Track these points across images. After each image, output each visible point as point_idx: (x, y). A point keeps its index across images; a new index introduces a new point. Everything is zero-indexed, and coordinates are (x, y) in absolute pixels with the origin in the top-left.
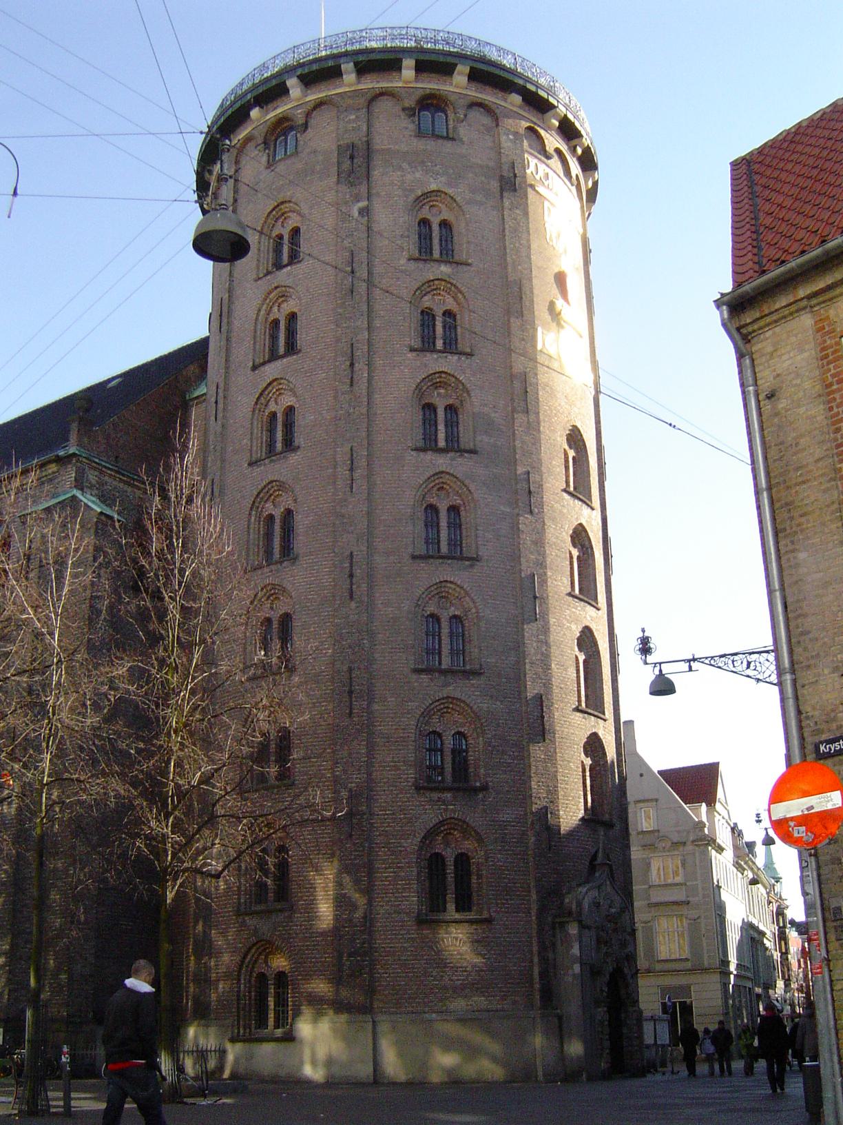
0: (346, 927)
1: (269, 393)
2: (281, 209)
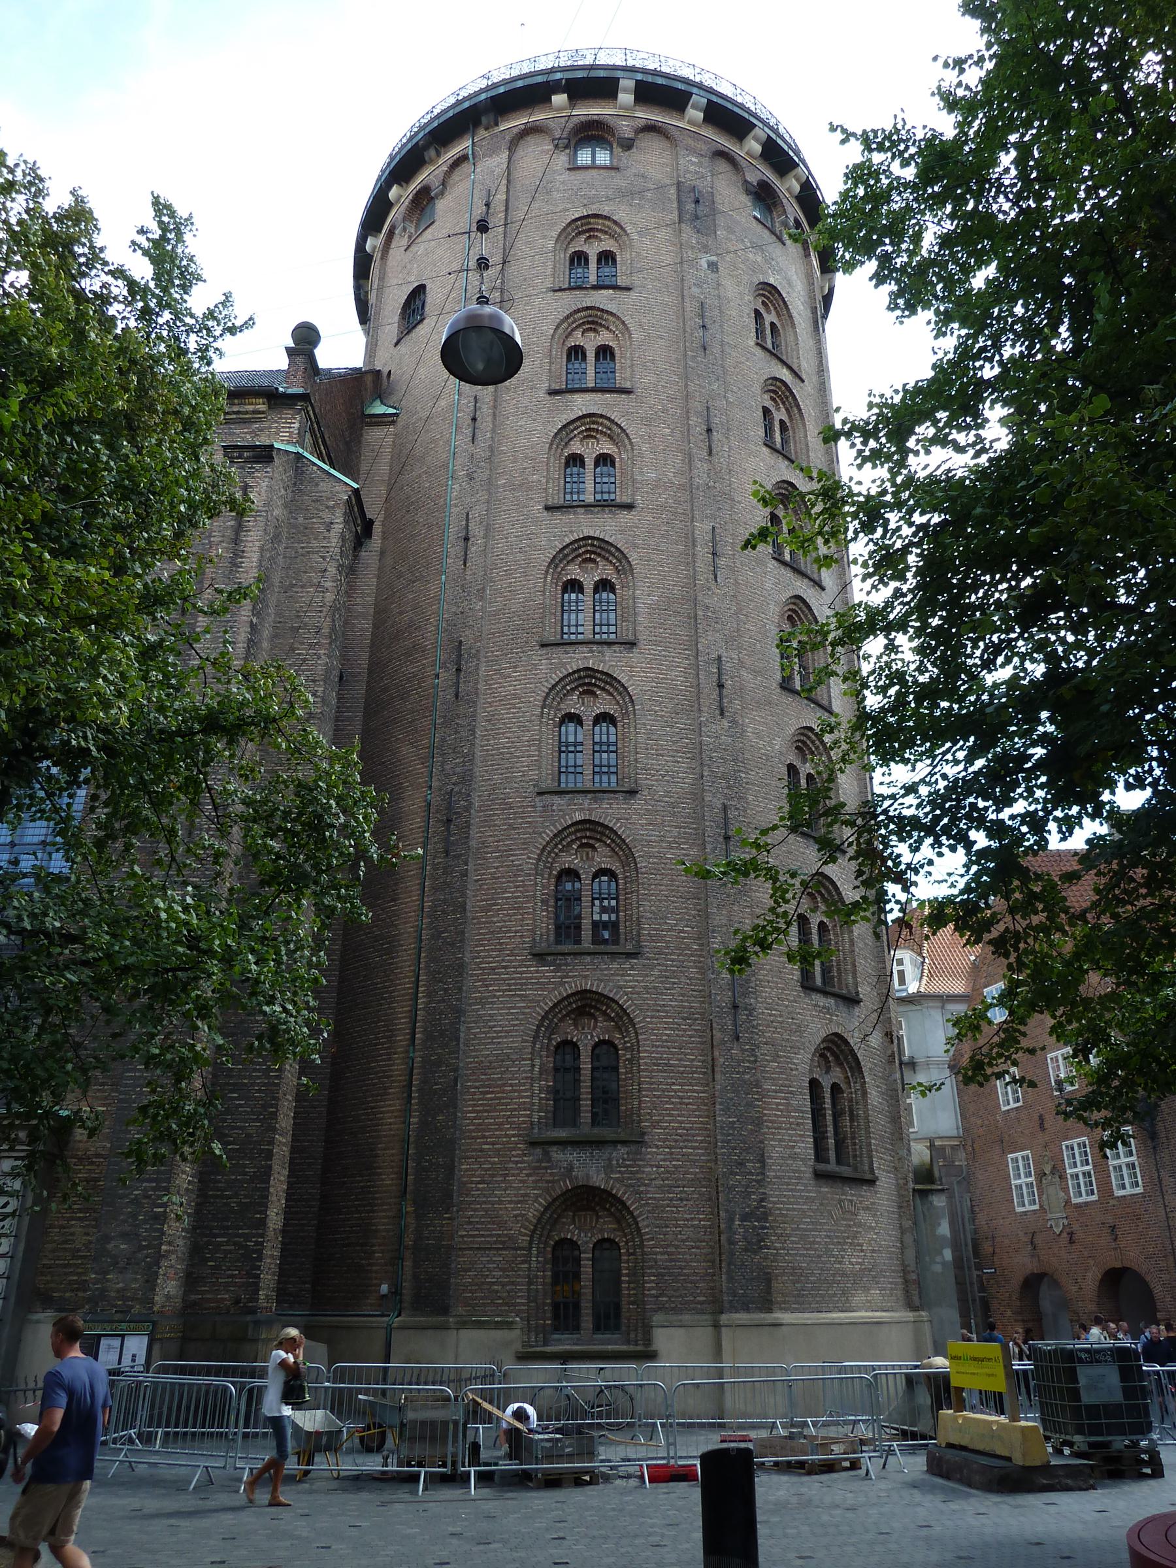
0: (736, 1174)
1: (575, 429)
2: (590, 223)
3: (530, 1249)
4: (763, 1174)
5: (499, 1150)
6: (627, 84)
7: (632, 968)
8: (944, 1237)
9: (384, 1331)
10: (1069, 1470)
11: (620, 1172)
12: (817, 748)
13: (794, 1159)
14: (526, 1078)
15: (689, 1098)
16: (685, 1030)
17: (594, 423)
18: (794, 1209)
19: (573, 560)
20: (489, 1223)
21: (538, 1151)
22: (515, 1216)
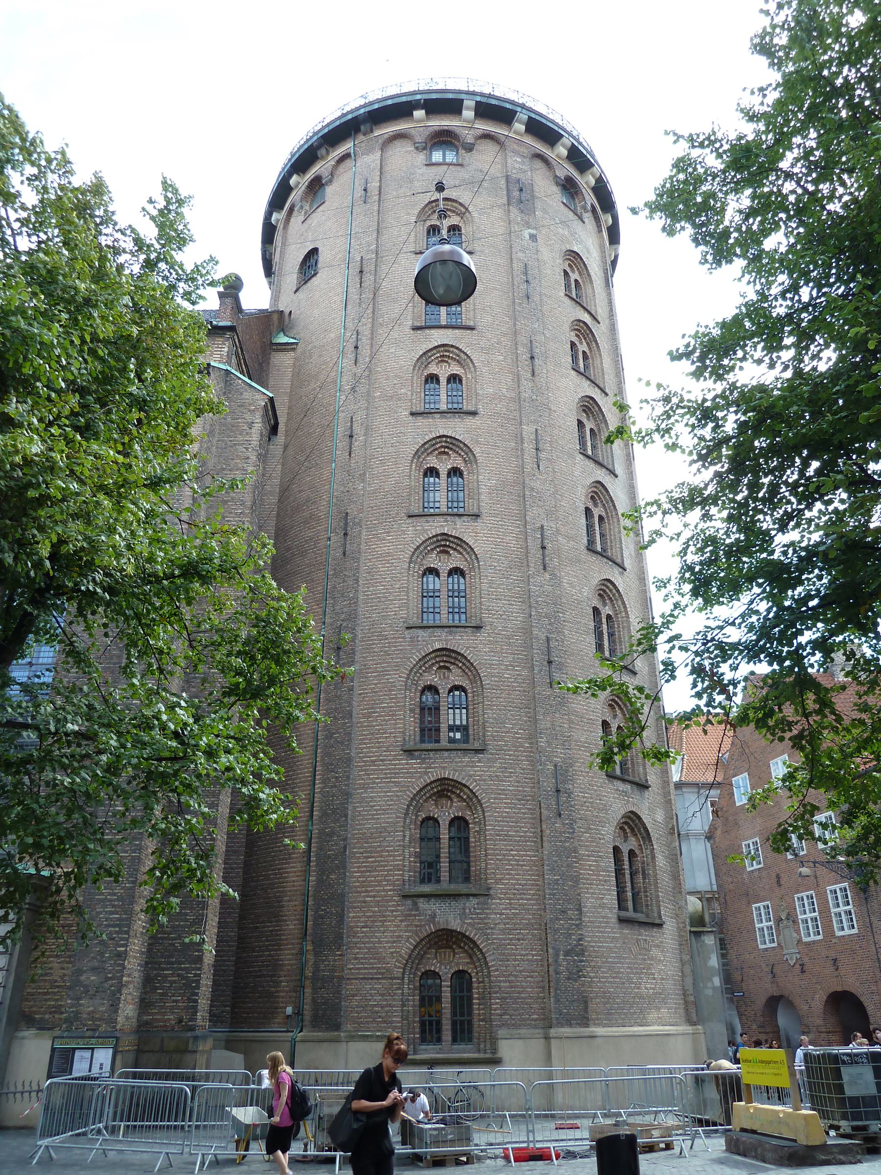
0: (561, 919)
3: (403, 978)
4: (580, 919)
5: (378, 901)
6: (469, 103)
7: (479, 761)
8: (713, 967)
9: (288, 1044)
10: (845, 1150)
11: (471, 918)
12: (614, 595)
13: (603, 908)
14: (399, 846)
15: (523, 861)
16: (520, 809)
17: (446, 351)
18: (603, 947)
19: (431, 453)
20: (371, 958)
21: (409, 902)
22: (392, 953)
